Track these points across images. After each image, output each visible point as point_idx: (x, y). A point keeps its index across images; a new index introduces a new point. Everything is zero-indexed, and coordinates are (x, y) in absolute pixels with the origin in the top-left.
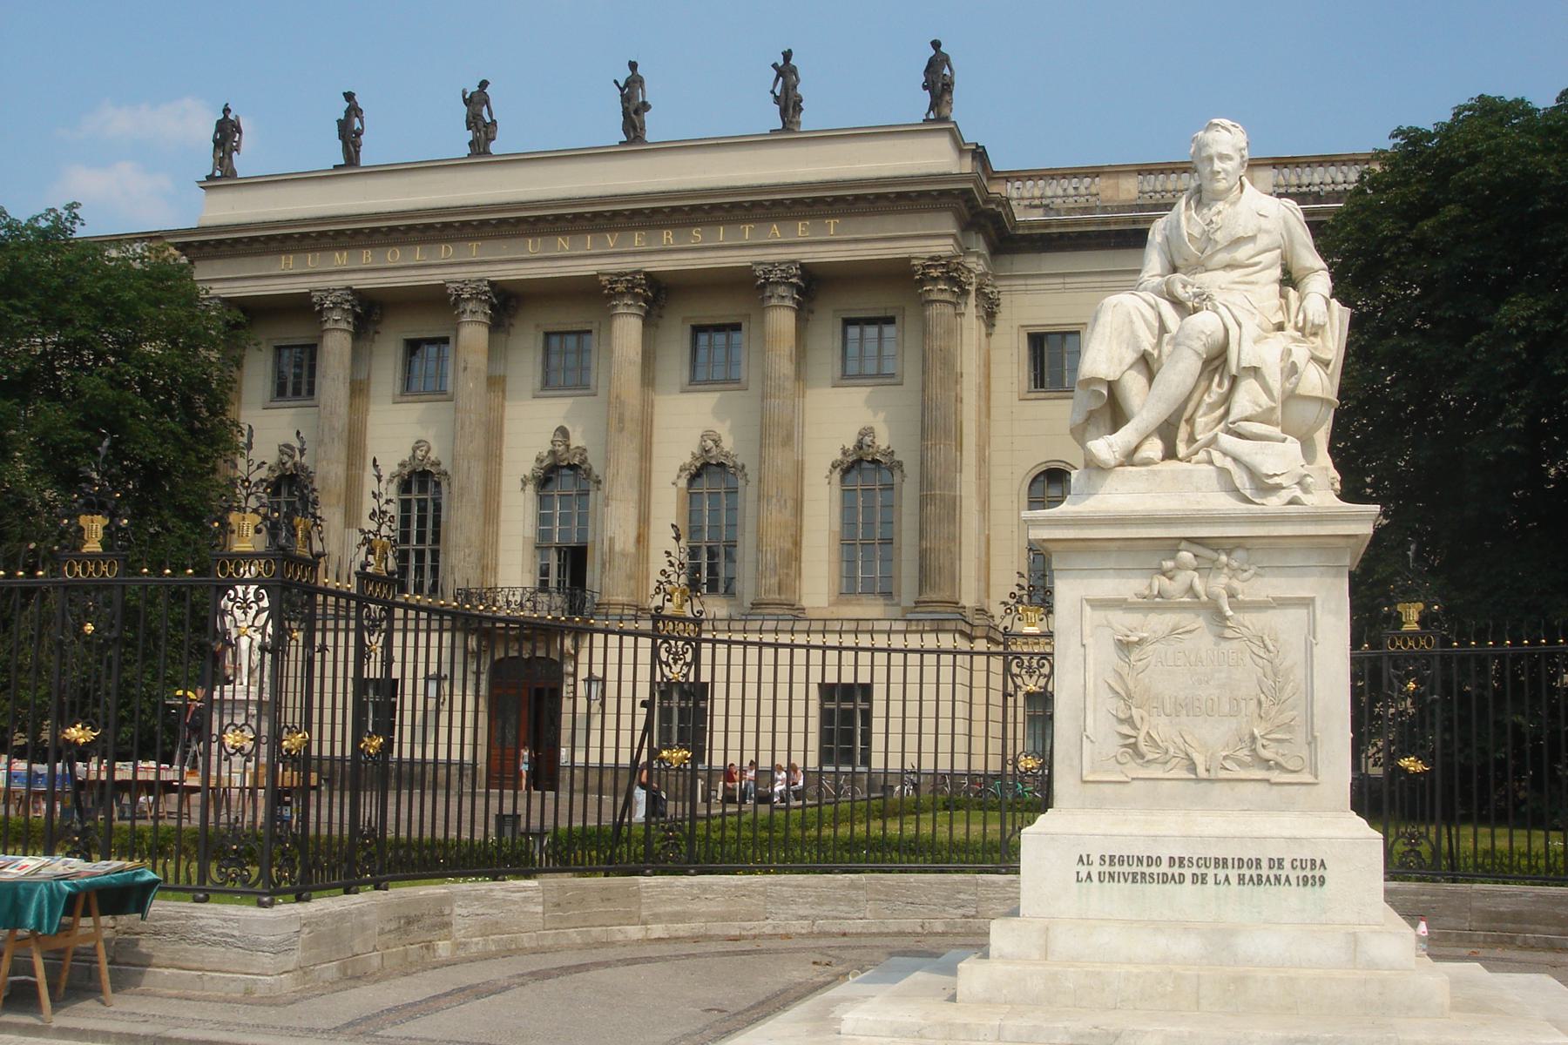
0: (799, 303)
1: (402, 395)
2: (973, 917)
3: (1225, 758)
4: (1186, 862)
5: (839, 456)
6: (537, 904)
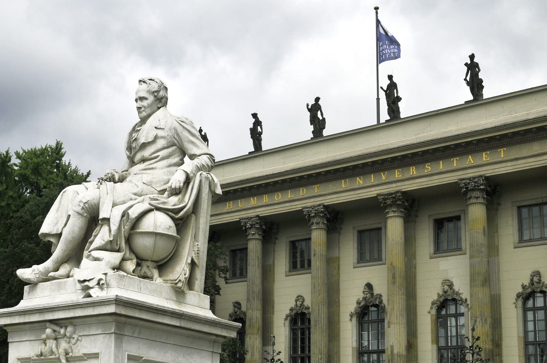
0: (487, 200)
1: (290, 271)
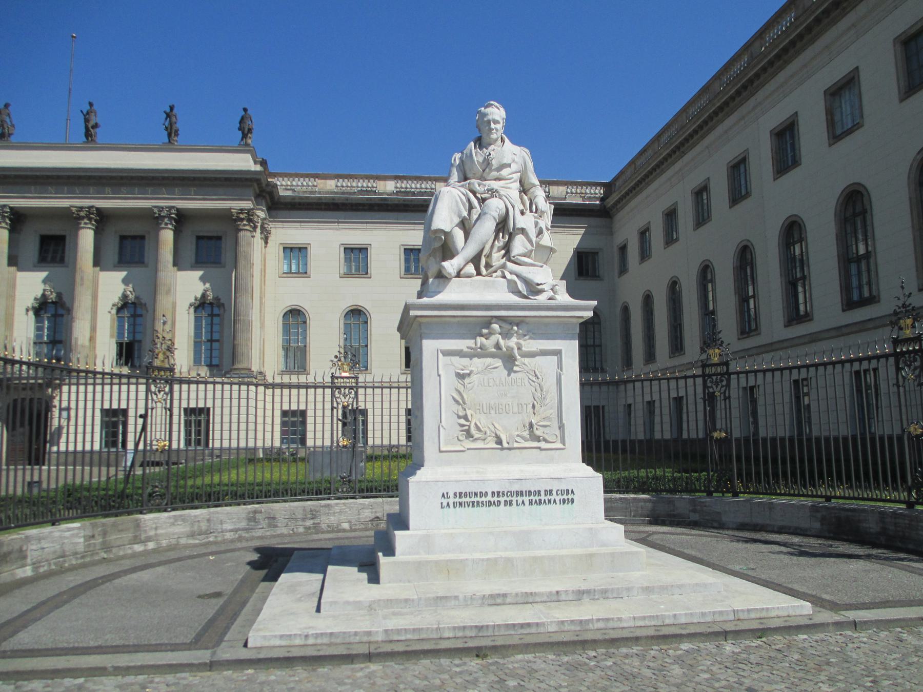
0: (175, 227)
2: (319, 524)
3: (518, 436)
5: (193, 301)
6: (80, 537)
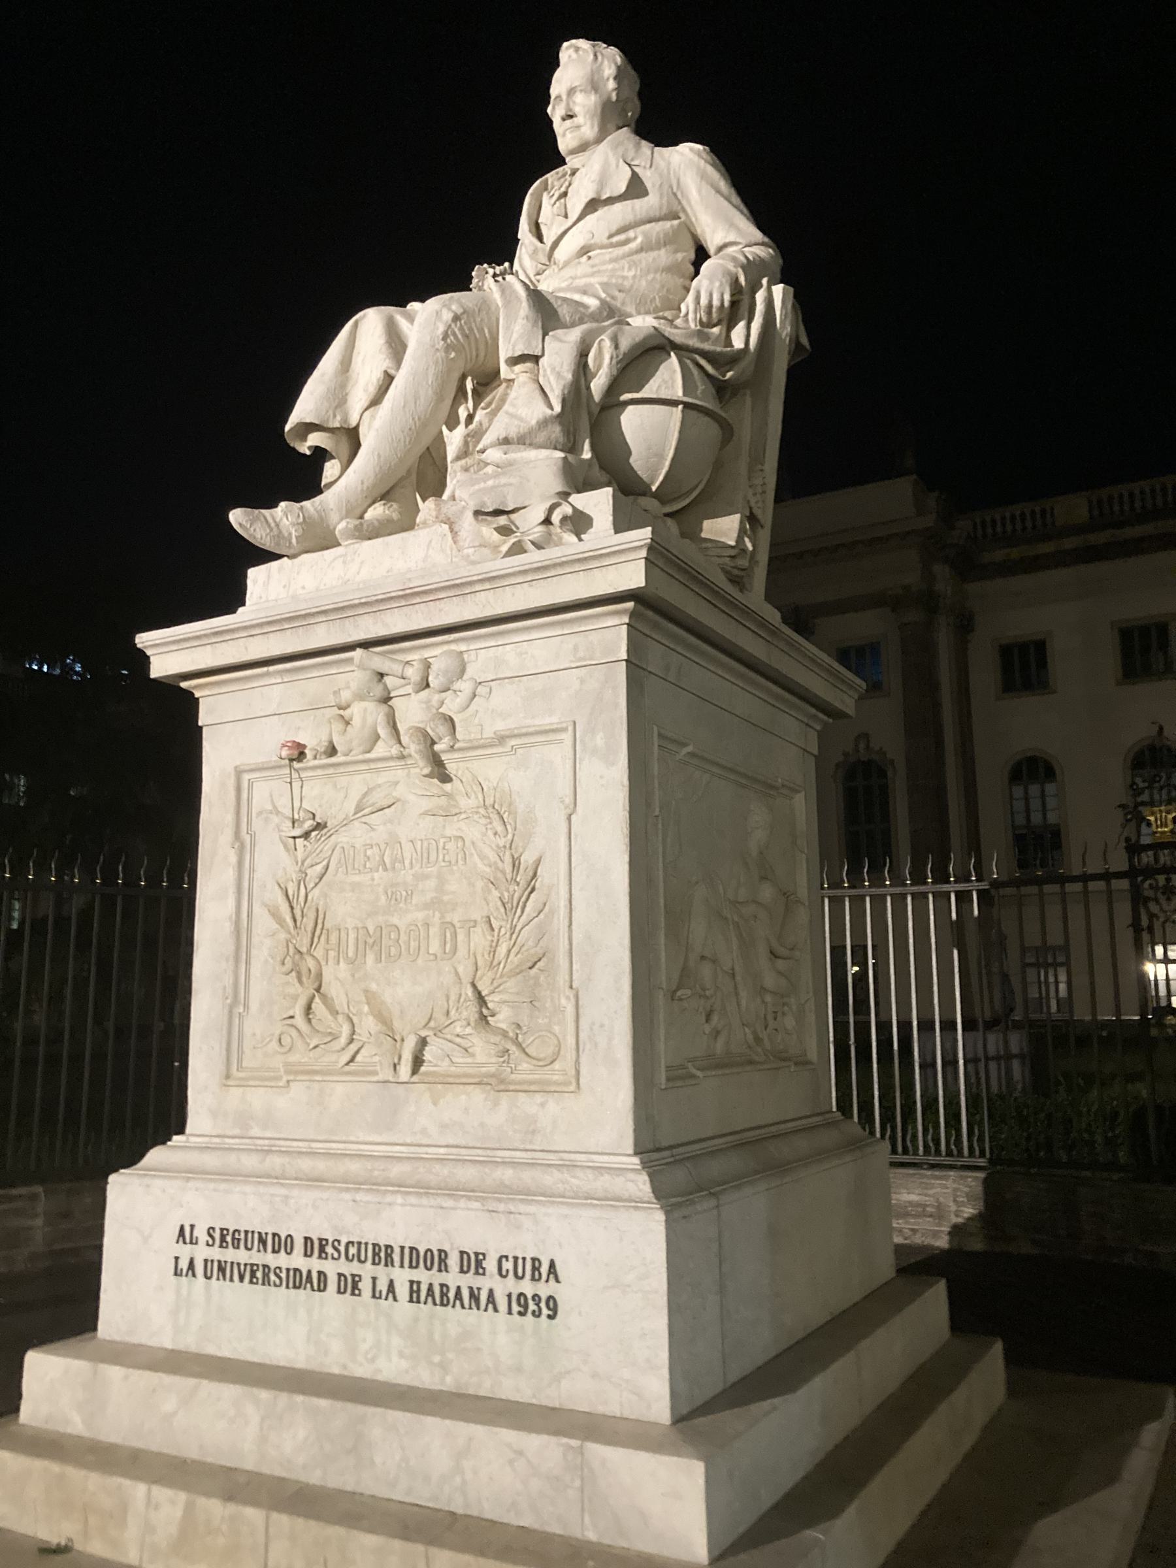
4: (329, 1250)
5: (841, 758)
